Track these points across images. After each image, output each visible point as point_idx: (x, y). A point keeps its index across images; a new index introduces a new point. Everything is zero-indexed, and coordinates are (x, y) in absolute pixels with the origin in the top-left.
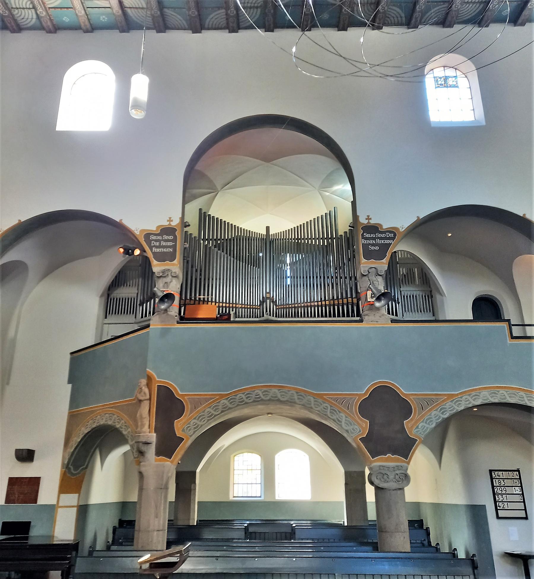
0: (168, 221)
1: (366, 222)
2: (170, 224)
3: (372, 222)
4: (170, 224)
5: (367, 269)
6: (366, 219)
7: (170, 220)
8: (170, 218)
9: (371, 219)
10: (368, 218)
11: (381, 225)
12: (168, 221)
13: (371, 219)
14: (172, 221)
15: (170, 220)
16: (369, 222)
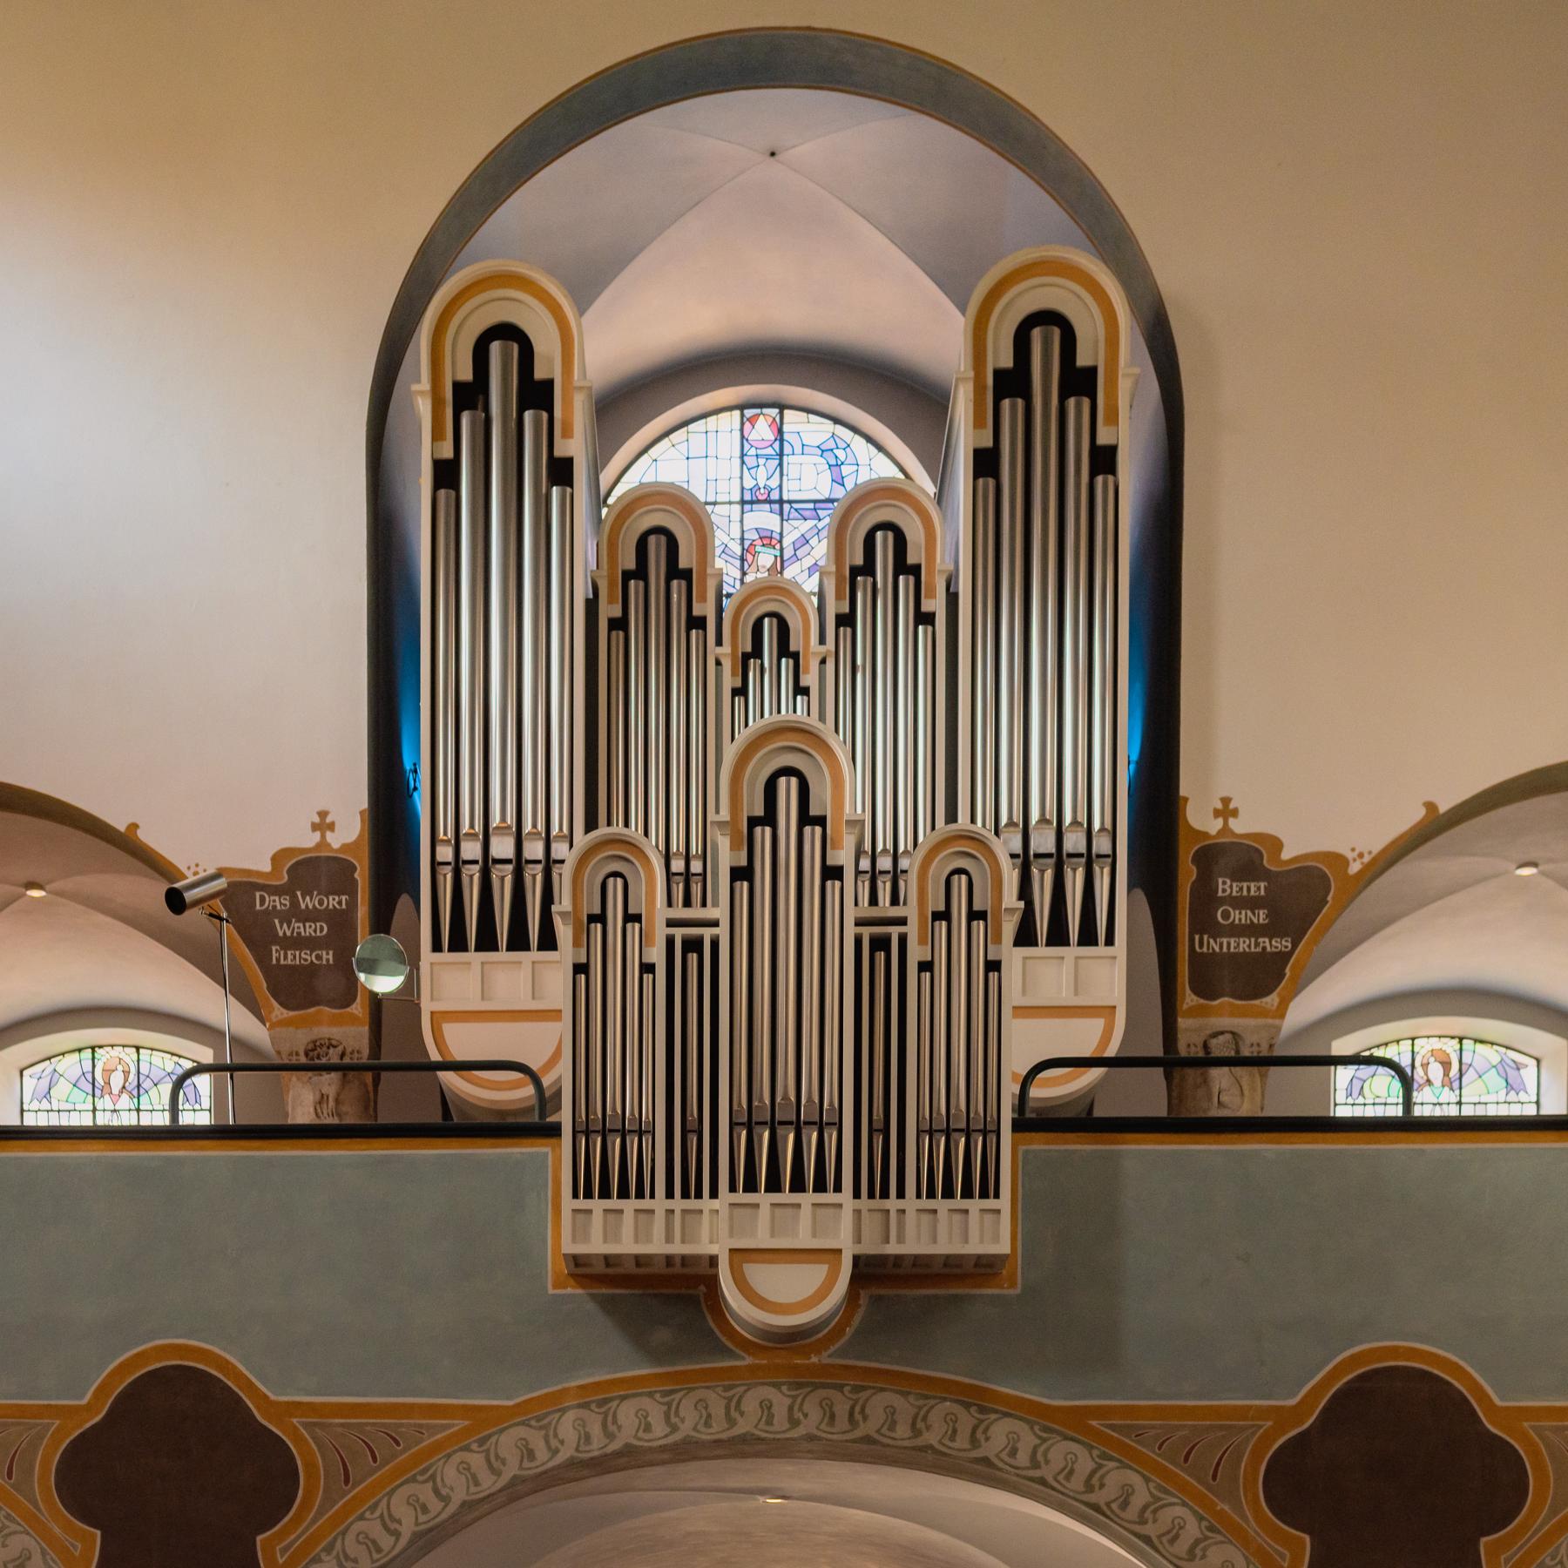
0: (315, 827)
1: (1213, 826)
2: (323, 844)
3: (1239, 826)
4: (323, 844)
5: (1199, 1040)
6: (1217, 813)
7: (323, 824)
8: (323, 814)
9: (1235, 813)
10: (1226, 811)
11: (1276, 844)
12: (315, 827)
13: (1235, 813)
14: (331, 827)
15: (323, 824)
16: (1225, 829)
